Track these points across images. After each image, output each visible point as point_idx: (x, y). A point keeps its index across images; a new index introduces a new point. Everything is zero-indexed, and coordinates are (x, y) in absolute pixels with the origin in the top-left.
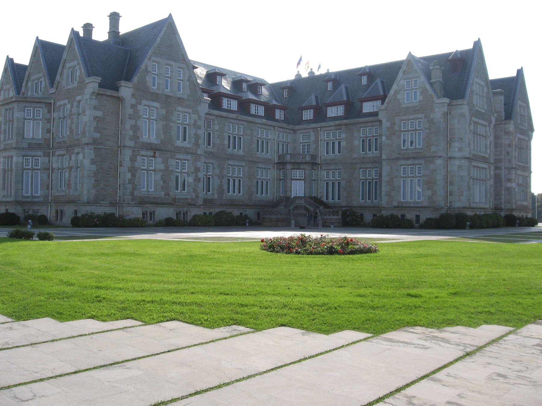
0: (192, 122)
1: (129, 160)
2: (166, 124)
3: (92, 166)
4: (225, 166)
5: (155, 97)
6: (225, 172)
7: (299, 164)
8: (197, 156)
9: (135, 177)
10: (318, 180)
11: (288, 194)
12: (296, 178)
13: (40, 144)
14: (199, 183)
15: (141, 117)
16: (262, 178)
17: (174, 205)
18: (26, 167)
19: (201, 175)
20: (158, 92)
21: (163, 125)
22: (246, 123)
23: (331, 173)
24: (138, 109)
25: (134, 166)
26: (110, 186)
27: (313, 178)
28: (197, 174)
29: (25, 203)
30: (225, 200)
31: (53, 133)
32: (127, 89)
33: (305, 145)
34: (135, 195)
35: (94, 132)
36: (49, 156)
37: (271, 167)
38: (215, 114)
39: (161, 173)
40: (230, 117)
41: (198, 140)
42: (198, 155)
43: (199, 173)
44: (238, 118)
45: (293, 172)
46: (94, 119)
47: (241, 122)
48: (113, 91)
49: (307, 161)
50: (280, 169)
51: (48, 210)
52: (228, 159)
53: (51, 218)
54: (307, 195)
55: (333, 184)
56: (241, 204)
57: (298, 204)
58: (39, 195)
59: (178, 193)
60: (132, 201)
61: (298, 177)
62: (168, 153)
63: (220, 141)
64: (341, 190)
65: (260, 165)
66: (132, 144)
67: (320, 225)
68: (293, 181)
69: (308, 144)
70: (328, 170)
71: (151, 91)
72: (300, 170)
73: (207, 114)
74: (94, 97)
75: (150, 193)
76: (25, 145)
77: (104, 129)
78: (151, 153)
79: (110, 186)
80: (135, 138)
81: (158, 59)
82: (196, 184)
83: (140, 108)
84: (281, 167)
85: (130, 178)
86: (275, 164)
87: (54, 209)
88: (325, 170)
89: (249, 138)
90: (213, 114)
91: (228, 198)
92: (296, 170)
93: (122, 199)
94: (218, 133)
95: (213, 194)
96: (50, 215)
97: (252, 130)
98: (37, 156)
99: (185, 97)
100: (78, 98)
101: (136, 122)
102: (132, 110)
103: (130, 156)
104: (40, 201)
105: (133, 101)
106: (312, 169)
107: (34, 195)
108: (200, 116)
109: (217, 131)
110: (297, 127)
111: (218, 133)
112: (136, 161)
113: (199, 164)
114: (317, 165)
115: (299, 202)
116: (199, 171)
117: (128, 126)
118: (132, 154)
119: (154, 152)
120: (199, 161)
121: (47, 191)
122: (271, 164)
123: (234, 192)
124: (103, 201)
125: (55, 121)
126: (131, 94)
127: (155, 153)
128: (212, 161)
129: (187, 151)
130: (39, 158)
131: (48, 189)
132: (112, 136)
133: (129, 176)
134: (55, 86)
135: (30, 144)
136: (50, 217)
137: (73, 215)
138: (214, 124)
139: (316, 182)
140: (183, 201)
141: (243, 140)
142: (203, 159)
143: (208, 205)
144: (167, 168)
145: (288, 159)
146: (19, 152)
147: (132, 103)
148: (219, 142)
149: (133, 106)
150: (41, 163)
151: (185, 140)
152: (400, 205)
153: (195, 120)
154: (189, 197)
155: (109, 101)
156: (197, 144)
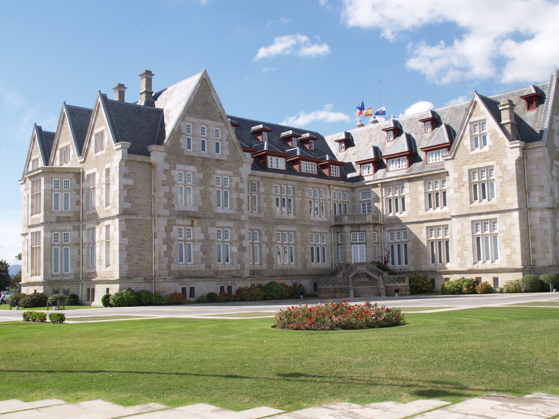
0: (234, 185)
1: (163, 230)
2: (205, 189)
3: (124, 239)
5: (191, 160)
7: (359, 225)
10: (382, 242)
11: (348, 261)
12: (356, 242)
13: (69, 217)
15: (176, 183)
16: (318, 243)
17: (217, 278)
18: (55, 243)
19: (246, 243)
20: (194, 155)
23: (395, 234)
24: (172, 175)
25: (170, 237)
26: (145, 260)
27: (376, 241)
28: (242, 242)
29: (55, 282)
30: (276, 270)
31: (83, 205)
33: (365, 204)
35: (125, 201)
36: (79, 230)
37: (327, 231)
38: (260, 175)
39: (200, 244)
40: (278, 177)
41: (241, 206)
42: (242, 221)
43: (243, 241)
46: (124, 188)
47: (290, 182)
48: (143, 157)
49: (367, 222)
50: (338, 233)
51: (79, 288)
52: (277, 224)
53: (83, 298)
54: (370, 260)
55: (399, 246)
56: (294, 274)
57: (359, 271)
58: (69, 272)
59: (221, 266)
60: (169, 276)
61: (358, 240)
63: (267, 205)
64: (409, 253)
65: (314, 230)
67: (383, 294)
68: (352, 245)
70: (392, 231)
72: (360, 233)
73: (250, 175)
75: (189, 266)
76: (54, 219)
77: (136, 198)
79: (145, 260)
80: (170, 206)
81: (193, 119)
83: (174, 173)
84: (338, 230)
86: (331, 227)
87: (85, 287)
88: (388, 231)
89: (300, 199)
90: (257, 175)
91: (279, 268)
92: (355, 233)
93: (158, 275)
94: (264, 196)
96: (82, 295)
98: (66, 231)
99: (224, 158)
100: (107, 166)
101: (170, 188)
102: (166, 176)
104: (70, 280)
105: (167, 166)
106: (374, 231)
107: (64, 273)
108: (242, 178)
109: (263, 193)
112: (172, 231)
113: (243, 232)
114: (380, 226)
115: (361, 269)
116: (244, 239)
117: (162, 194)
120: (243, 228)
121: (79, 268)
124: (137, 277)
125: (85, 192)
126: (164, 159)
127: (192, 221)
128: (259, 227)
129: (229, 218)
130: (69, 232)
131: (79, 266)
133: (164, 248)
134: (83, 154)
135: (58, 218)
136: (82, 297)
137: (105, 294)
138: (259, 186)
139: (379, 245)
140: (226, 273)
141: (294, 203)
142: (247, 226)
143: (255, 276)
144: (207, 238)
145: (346, 221)
147: (165, 168)
148: (266, 206)
149: (166, 172)
150: (71, 237)
153: (236, 183)
154: (233, 269)
156: (240, 209)
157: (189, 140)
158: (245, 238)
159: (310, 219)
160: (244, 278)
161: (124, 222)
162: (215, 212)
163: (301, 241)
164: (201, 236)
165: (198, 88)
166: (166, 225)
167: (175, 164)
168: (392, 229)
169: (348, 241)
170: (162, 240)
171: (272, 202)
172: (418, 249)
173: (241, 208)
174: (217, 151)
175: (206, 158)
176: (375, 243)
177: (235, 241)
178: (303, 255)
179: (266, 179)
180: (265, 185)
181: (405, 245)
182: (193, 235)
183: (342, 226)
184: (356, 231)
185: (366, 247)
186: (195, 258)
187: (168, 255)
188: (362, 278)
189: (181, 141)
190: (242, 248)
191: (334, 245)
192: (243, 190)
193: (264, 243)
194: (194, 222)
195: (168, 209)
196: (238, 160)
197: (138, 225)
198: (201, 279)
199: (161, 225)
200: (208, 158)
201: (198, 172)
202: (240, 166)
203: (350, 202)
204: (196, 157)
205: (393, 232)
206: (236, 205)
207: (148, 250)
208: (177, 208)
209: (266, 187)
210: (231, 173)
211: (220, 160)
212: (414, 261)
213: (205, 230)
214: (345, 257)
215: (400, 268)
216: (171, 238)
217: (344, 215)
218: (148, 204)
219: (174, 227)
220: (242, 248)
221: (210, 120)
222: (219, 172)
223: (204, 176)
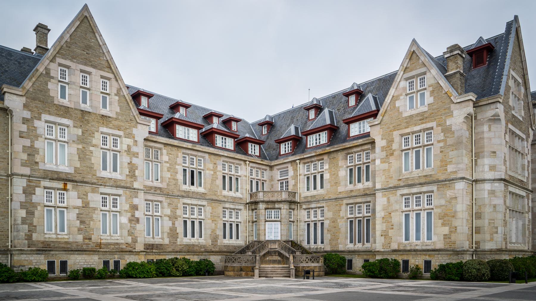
4: (179, 204)
7: (274, 202)
8: (133, 190)
10: (298, 221)
12: (270, 219)
14: (137, 225)
22: (207, 156)
23: (312, 212)
25: (31, 200)
27: (292, 220)
28: (135, 213)
33: (283, 182)
42: (134, 189)
43: (136, 212)
44: (195, 148)
50: (253, 210)
52: (183, 197)
54: (284, 239)
62: (87, 185)
63: (171, 175)
64: (325, 231)
65: (227, 205)
66: (27, 171)
69: (287, 180)
70: (309, 209)
72: (275, 210)
78: (61, 185)
82: (132, 225)
86: (246, 204)
88: (305, 209)
89: (212, 173)
92: (270, 210)
94: (168, 165)
97: (215, 164)
101: (32, 142)
106: (290, 209)
110: (273, 163)
113: (136, 201)
114: (297, 204)
116: (137, 209)
118: (27, 185)
119: (65, 183)
120: (136, 197)
122: (241, 203)
127: (65, 185)
128: (160, 198)
129: (117, 185)
138: (162, 154)
139: (295, 223)
141: (204, 176)
142: (141, 195)
144: (86, 205)
145: (260, 198)
151: (115, 170)
152: (401, 248)
158: (139, 208)
159: (223, 195)
162: (97, 176)
163: (211, 216)
164: (79, 203)
166: (25, 185)
168: (309, 207)
169: (262, 218)
171: (177, 173)
172: (335, 227)
173: (135, 175)
176: (290, 221)
178: (213, 231)
180: (168, 154)
181: (322, 224)
182: (67, 201)
183: (256, 203)
185: (281, 224)
186: (69, 227)
188: (274, 257)
191: (249, 222)
193: (165, 215)
194: (68, 185)
203: (267, 180)
205: (310, 210)
206: (128, 170)
209: (170, 155)
212: (330, 240)
213: (83, 197)
214: (259, 235)
215: (316, 247)
219: (37, 189)
221: (93, 68)
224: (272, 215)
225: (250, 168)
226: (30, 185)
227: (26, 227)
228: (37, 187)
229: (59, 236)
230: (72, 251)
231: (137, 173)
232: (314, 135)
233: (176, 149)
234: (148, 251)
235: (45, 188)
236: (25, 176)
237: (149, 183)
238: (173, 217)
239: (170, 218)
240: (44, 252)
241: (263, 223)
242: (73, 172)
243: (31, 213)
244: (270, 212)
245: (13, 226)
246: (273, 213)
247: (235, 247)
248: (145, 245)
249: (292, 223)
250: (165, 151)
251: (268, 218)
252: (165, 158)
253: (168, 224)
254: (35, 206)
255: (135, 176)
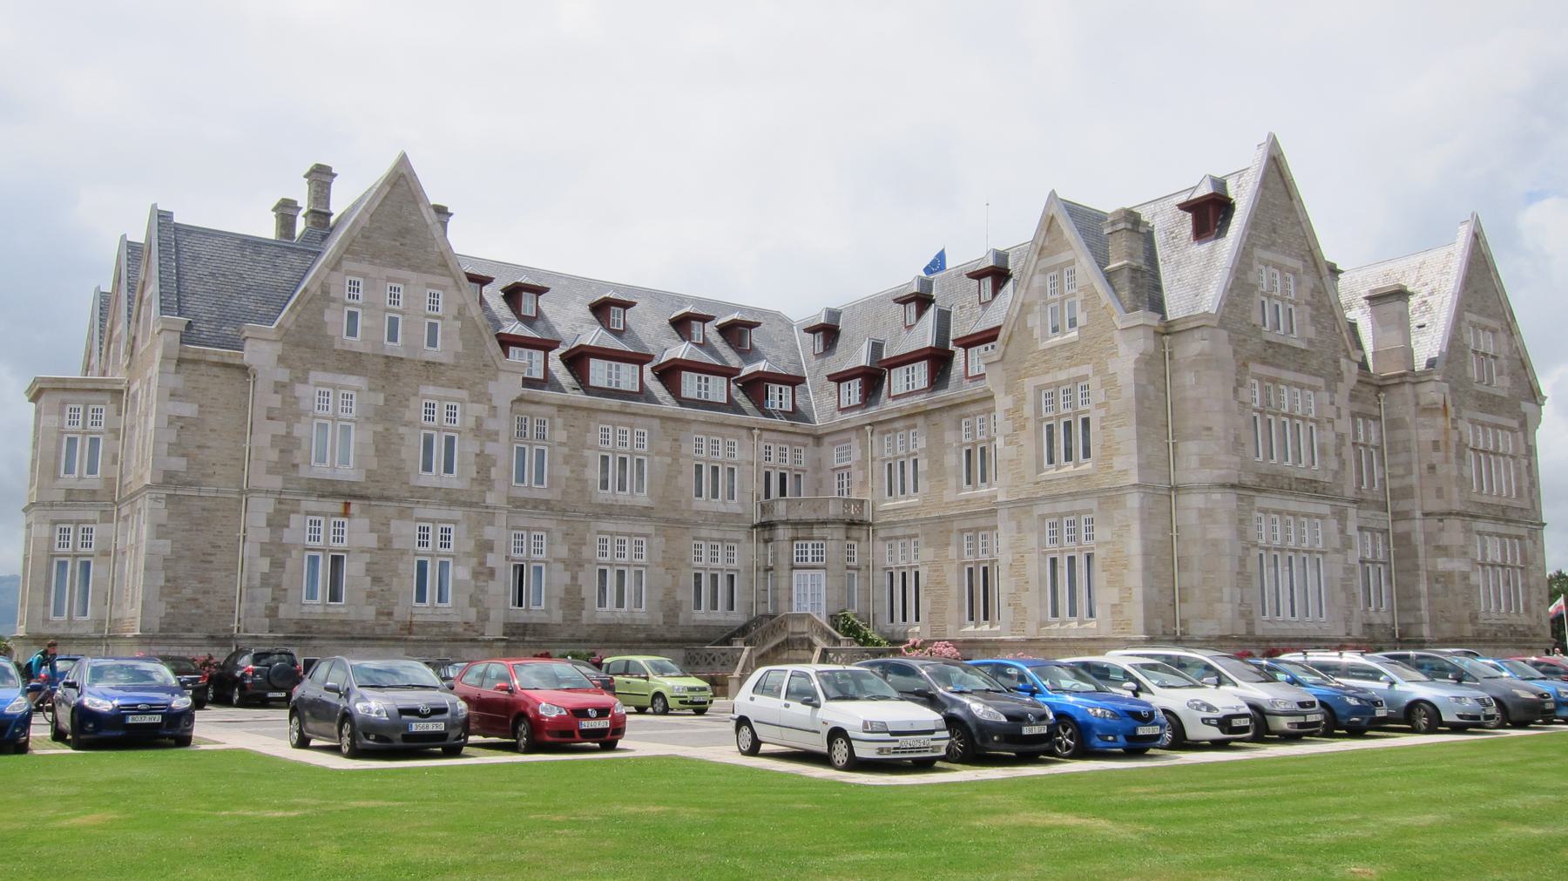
0: (471, 422)
4: (588, 535)
5: (353, 362)
6: (586, 552)
7: (809, 524)
9: (284, 567)
10: (868, 566)
15: (307, 416)
21: (375, 432)
22: (656, 423)
24: (297, 394)
27: (855, 564)
28: (486, 557)
30: (588, 625)
32: (263, 345)
34: (280, 616)
39: (367, 557)
40: (603, 407)
41: (489, 470)
42: (487, 507)
44: (628, 410)
45: (797, 547)
46: (170, 423)
50: (766, 542)
52: (597, 516)
56: (642, 636)
57: (793, 633)
62: (390, 504)
63: (572, 471)
65: (704, 533)
68: (795, 573)
70: (890, 538)
71: (337, 346)
72: (815, 542)
73: (520, 400)
74: (172, 368)
78: (337, 506)
80: (286, 463)
81: (365, 267)
82: (479, 584)
85: (267, 571)
88: (885, 539)
89: (669, 460)
91: (598, 622)
92: (804, 542)
94: (566, 450)
95: (548, 611)
97: (676, 440)
98: (86, 522)
102: (279, 397)
103: (268, 514)
105: (283, 375)
109: (561, 444)
111: (566, 450)
113: (489, 533)
114: (865, 528)
115: (796, 630)
116: (491, 549)
118: (275, 510)
119: (346, 503)
120: (491, 523)
122: (739, 527)
123: (620, 604)
127: (347, 505)
128: (546, 524)
129: (450, 498)
132: (226, 465)
133: (264, 565)
138: (552, 428)
140: (436, 630)
144: (385, 544)
146: (45, 512)
149: (280, 387)
151: (449, 468)
155: (218, 377)
156: (484, 479)
157: (353, 316)
159: (694, 508)
160: (484, 641)
161: (163, 501)
163: (663, 558)
164: (371, 541)
165: (382, 196)
167: (306, 371)
169: (784, 561)
170: (258, 547)
171: (586, 466)
173: (489, 477)
174: (432, 342)
175: (394, 358)
176: (848, 568)
177: (464, 553)
178: (669, 593)
179: (572, 411)
182: (349, 538)
183: (768, 526)
184: (803, 539)
187: (273, 581)
189: (327, 318)
190: (486, 571)
192: (497, 433)
193: (556, 560)
195: (278, 474)
196: (484, 365)
197: (204, 510)
198: (362, 642)
199: (258, 512)
200: (401, 359)
201: (370, 390)
202: (491, 380)
204: (367, 355)
206: (475, 468)
207: (225, 570)
208: (304, 472)
210: (464, 394)
211: (434, 363)
213: (381, 528)
216: (284, 541)
217: (777, 500)
218: (232, 462)
220: (486, 571)
222: (429, 390)
223: (386, 400)
224: (807, 553)
225: (762, 444)
226: (280, 510)
227: (268, 591)
228: (294, 512)
229: (330, 610)
230: (353, 638)
231: (494, 473)
232: (904, 368)
233: (585, 413)
234: (513, 639)
235: (308, 513)
236: (273, 492)
237: (521, 492)
238: (575, 564)
239: (567, 564)
240: (298, 642)
241: (786, 573)
242: (363, 479)
243: (278, 565)
244: (802, 547)
245: (244, 590)
246: (810, 550)
247: (703, 627)
248: (506, 625)
249: (855, 572)
250: (559, 421)
251: (797, 560)
252: (561, 435)
253: (562, 578)
254: (286, 549)
255: (490, 481)
